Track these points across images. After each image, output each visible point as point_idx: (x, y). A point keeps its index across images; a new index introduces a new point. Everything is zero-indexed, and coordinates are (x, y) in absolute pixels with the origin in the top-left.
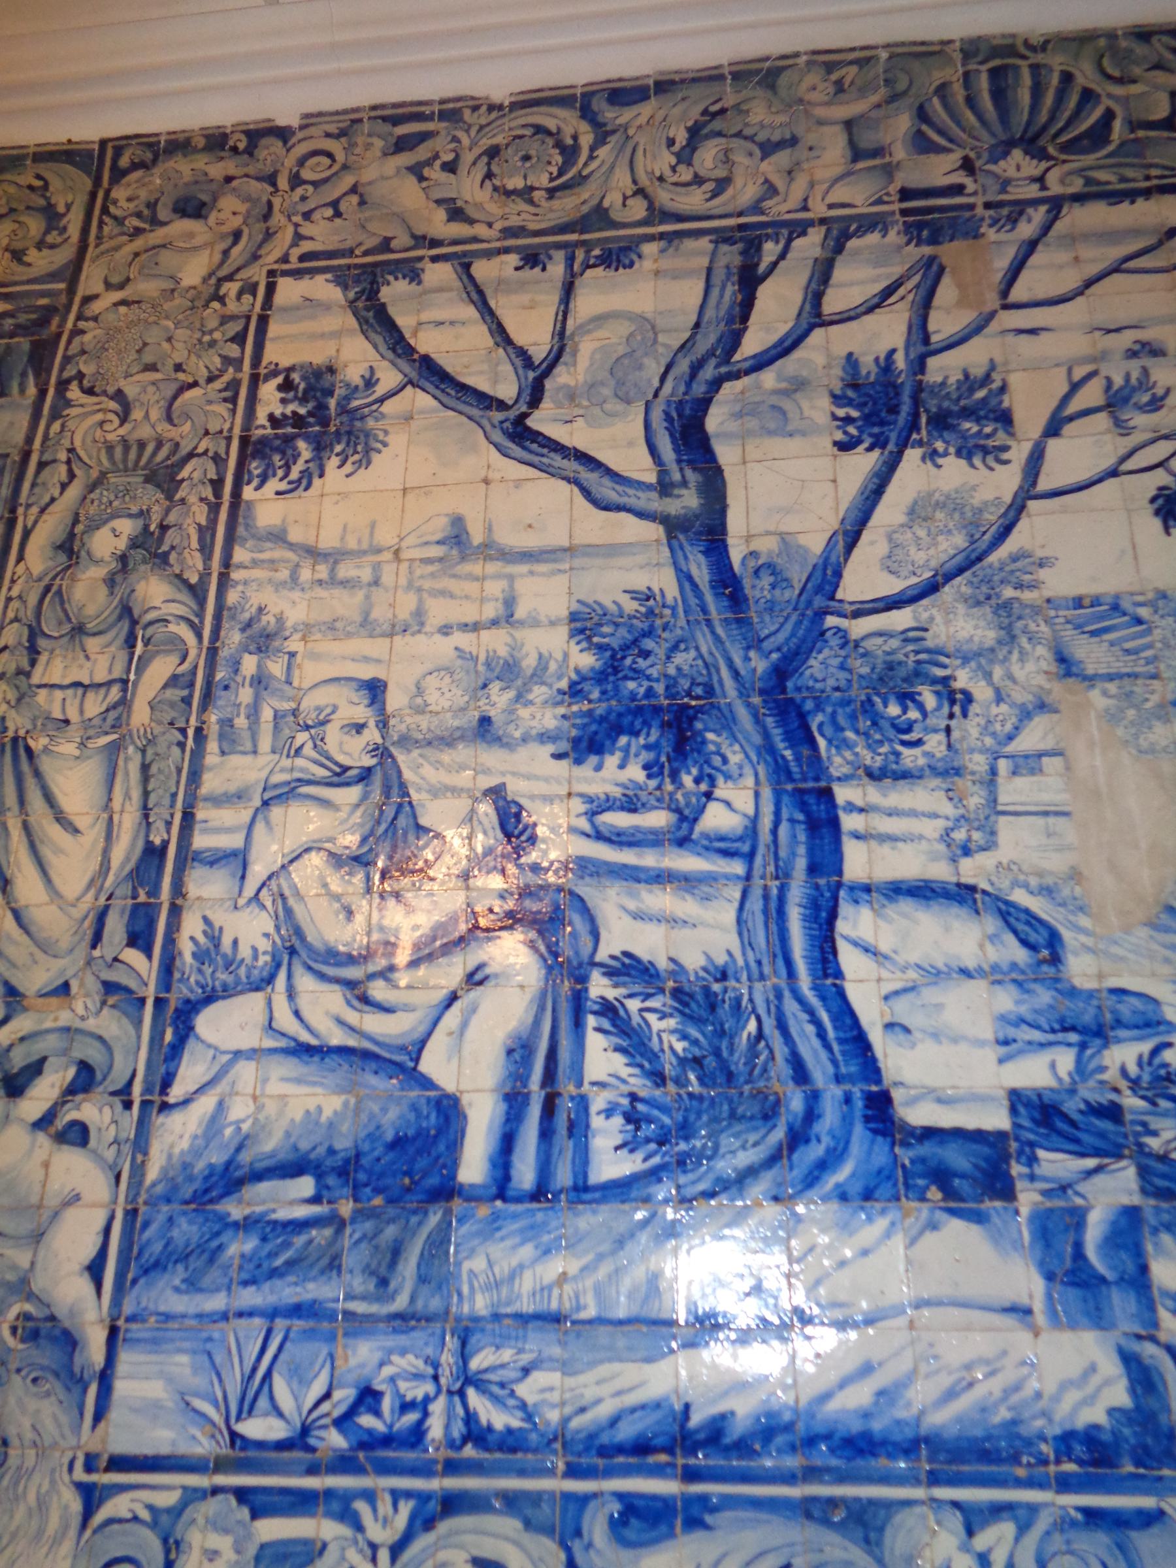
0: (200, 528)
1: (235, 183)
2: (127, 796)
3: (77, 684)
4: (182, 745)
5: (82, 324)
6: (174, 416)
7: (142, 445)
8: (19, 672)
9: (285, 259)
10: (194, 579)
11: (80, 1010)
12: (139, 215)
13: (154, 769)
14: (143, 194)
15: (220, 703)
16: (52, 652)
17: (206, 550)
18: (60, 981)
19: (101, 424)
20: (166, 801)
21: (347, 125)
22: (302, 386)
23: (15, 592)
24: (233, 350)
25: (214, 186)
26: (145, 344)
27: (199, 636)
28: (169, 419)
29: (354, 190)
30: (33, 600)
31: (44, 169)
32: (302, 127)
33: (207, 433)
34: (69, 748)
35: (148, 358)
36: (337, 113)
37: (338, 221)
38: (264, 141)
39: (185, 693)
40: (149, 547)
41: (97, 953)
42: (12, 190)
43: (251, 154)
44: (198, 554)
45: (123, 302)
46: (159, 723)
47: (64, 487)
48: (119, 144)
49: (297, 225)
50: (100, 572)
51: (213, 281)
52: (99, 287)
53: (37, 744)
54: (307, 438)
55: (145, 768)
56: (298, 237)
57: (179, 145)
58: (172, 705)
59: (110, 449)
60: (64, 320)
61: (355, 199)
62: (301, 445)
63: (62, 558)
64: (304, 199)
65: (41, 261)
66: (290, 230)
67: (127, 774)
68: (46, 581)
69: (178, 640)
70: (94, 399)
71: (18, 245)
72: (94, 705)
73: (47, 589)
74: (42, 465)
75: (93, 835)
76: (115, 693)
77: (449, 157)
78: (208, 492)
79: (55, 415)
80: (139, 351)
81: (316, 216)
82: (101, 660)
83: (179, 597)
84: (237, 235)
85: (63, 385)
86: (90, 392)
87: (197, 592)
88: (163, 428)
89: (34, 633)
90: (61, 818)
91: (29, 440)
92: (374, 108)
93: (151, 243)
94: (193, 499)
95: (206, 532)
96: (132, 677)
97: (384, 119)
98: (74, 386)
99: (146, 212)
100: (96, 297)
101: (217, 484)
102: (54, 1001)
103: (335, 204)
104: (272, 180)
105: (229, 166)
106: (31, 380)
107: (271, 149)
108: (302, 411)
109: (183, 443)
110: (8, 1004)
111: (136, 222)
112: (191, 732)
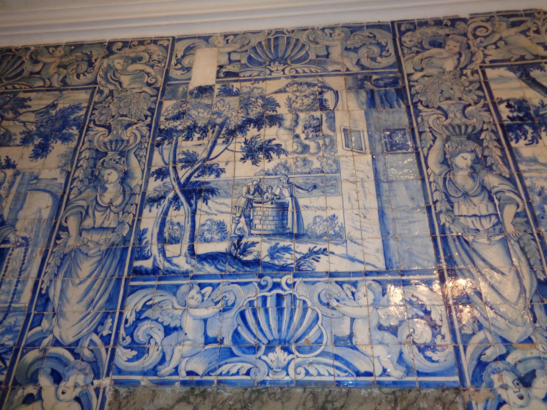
0: (500, 157)
1: (451, 36)
2: (519, 259)
3: (475, 216)
4: (534, 240)
5: (412, 83)
6: (467, 116)
7: (459, 127)
8: (448, 210)
9: (484, 62)
10: (508, 176)
11: (541, 349)
12: (416, 46)
13: (526, 249)
14: (415, 40)
15: (543, 223)
16: (458, 203)
17: (507, 165)
18: (526, 337)
19: (438, 118)
20: (538, 262)
21: (490, 17)
22: (516, 106)
23: (431, 179)
24: (480, 93)
25: (442, 37)
26: (442, 91)
27: (520, 196)
28: (465, 117)
29: (501, 39)
30: (441, 183)
31: (370, 30)
32: (471, 18)
33: (484, 122)
34: (484, 240)
35: (446, 95)
36: (486, 13)
37: (498, 50)
38: (458, 23)
39: (525, 219)
40: (481, 164)
41: (537, 325)
42: (361, 37)
43: (454, 27)
44: (504, 167)
45: (424, 76)
46: (520, 231)
47: (434, 141)
48: (400, 23)
49: (483, 51)
50: (466, 173)
51: (458, 69)
52: (412, 71)
53: (470, 238)
54: (528, 125)
55: (522, 249)
56: (485, 56)
57: (423, 23)
58: (522, 224)
59: (446, 128)
60: (403, 82)
61: (503, 43)
62: (527, 127)
63: (446, 167)
64: (481, 42)
65: (385, 62)
66: (481, 53)
67: (515, 251)
68: (443, 176)
69: (511, 201)
70: (430, 110)
71: (373, 56)
72: (487, 224)
73: (445, 179)
74: (420, 133)
75: (511, 275)
76: (494, 219)
77: (535, 29)
78: (496, 144)
79: (417, 116)
80: (441, 93)
81: (489, 47)
82: (482, 206)
83: (505, 182)
84: (460, 54)
85: (415, 105)
86: (427, 107)
87: (511, 180)
88: (464, 120)
89: (447, 196)
90: (493, 268)
91: (411, 124)
92: (498, 12)
93: (425, 56)
94: (491, 146)
95: (504, 158)
96: (499, 213)
97: (504, 16)
98: (419, 104)
99: (419, 46)
100: (413, 74)
101: (498, 140)
102: (526, 345)
103: (495, 44)
104: (465, 35)
105: (447, 31)
106: (401, 102)
107: (461, 26)
108: (521, 115)
109: (477, 126)
110: (506, 346)
111: (416, 49)
112: (536, 235)
